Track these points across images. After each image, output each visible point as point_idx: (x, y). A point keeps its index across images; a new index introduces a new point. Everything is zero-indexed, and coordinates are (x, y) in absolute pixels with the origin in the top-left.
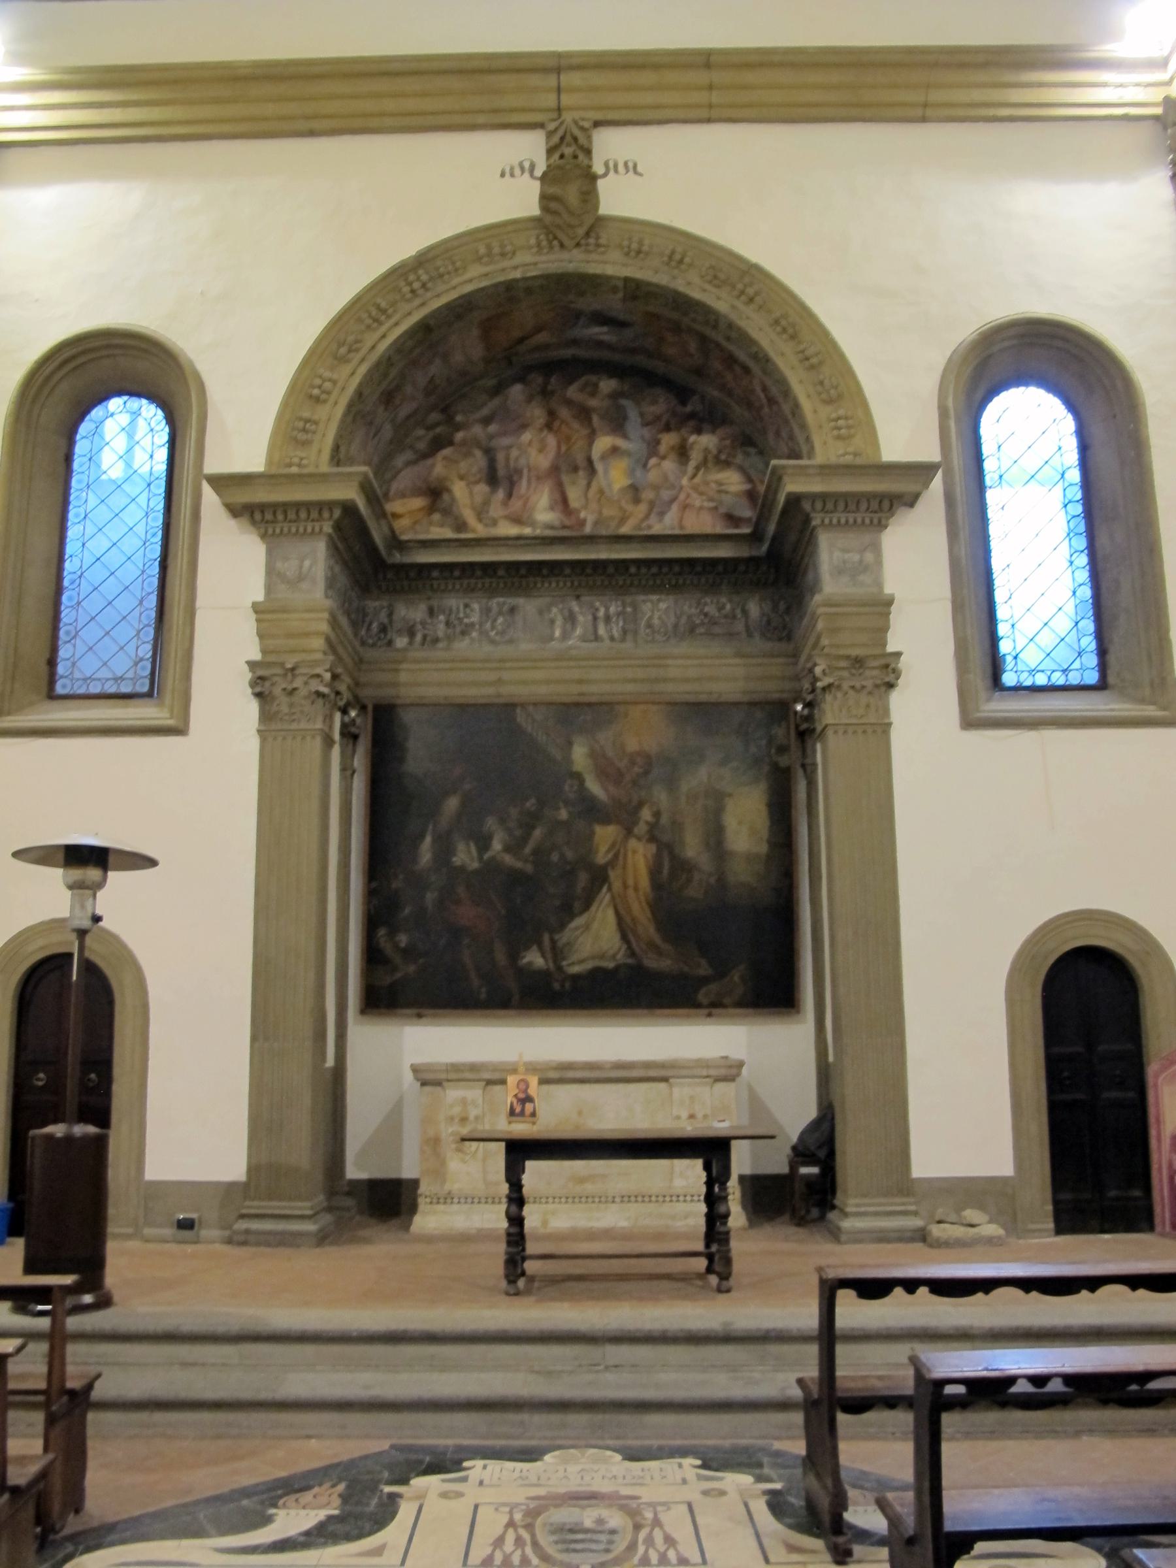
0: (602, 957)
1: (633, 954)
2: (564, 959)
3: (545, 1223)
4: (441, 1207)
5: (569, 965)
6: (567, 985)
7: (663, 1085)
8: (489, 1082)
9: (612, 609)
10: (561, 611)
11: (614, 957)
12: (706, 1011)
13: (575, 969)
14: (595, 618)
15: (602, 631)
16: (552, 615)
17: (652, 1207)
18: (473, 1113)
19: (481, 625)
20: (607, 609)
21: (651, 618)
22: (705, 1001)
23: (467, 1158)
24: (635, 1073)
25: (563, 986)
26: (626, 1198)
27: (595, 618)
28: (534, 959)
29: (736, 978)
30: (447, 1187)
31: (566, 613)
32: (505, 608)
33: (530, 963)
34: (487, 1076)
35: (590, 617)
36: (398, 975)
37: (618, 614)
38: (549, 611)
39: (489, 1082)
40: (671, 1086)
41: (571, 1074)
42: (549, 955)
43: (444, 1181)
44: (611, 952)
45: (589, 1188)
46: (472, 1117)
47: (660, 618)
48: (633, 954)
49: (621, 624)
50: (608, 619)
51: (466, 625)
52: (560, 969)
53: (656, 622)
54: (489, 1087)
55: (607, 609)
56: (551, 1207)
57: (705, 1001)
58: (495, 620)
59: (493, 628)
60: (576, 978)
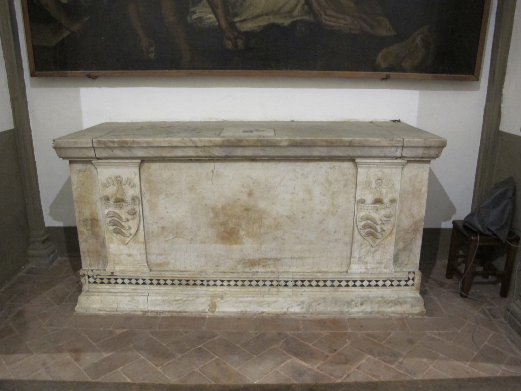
0: (276, 13)
1: (311, 10)
2: (236, 15)
3: (213, 306)
4: (105, 287)
5: (241, 21)
6: (240, 42)
7: (347, 165)
8: (143, 160)
11: (291, 12)
12: (384, 74)
13: (249, 26)
17: (327, 292)
18: (131, 192)
22: (383, 65)
23: (128, 239)
24: (316, 152)
25: (236, 45)
26: (299, 283)
28: (205, 15)
29: (418, 41)
30: (109, 268)
33: (200, 19)
34: (141, 153)
36: (66, 33)
39: (143, 160)
40: (356, 165)
41: (239, 152)
42: (220, 11)
43: (105, 261)
44: (287, 8)
45: (261, 272)
46: (128, 199)
48: (311, 10)
52: (232, 25)
54: (146, 165)
56: (219, 290)
57: (383, 65)
60: (248, 35)
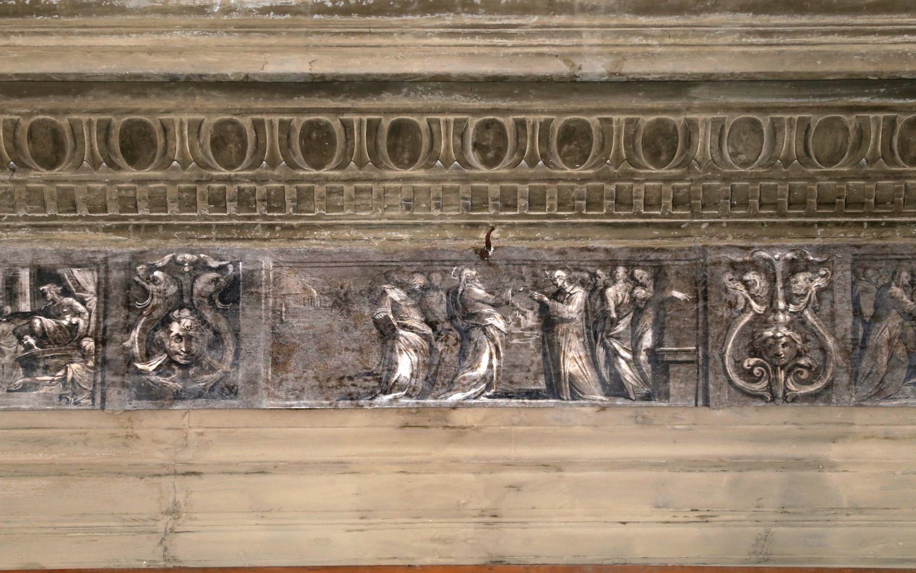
9: (615, 293)
10: (420, 298)
14: (549, 322)
15: (574, 361)
16: (384, 311)
19: (102, 342)
20: (596, 292)
21: (761, 321)
27: (549, 322)
31: (438, 303)
32: (203, 283)
35: (531, 319)
37: (637, 309)
38: (377, 297)
47: (797, 323)
49: (648, 340)
50: (597, 325)
51: (43, 337)
53: (780, 331)
55: (596, 292)
58: (166, 322)
59: (150, 349)
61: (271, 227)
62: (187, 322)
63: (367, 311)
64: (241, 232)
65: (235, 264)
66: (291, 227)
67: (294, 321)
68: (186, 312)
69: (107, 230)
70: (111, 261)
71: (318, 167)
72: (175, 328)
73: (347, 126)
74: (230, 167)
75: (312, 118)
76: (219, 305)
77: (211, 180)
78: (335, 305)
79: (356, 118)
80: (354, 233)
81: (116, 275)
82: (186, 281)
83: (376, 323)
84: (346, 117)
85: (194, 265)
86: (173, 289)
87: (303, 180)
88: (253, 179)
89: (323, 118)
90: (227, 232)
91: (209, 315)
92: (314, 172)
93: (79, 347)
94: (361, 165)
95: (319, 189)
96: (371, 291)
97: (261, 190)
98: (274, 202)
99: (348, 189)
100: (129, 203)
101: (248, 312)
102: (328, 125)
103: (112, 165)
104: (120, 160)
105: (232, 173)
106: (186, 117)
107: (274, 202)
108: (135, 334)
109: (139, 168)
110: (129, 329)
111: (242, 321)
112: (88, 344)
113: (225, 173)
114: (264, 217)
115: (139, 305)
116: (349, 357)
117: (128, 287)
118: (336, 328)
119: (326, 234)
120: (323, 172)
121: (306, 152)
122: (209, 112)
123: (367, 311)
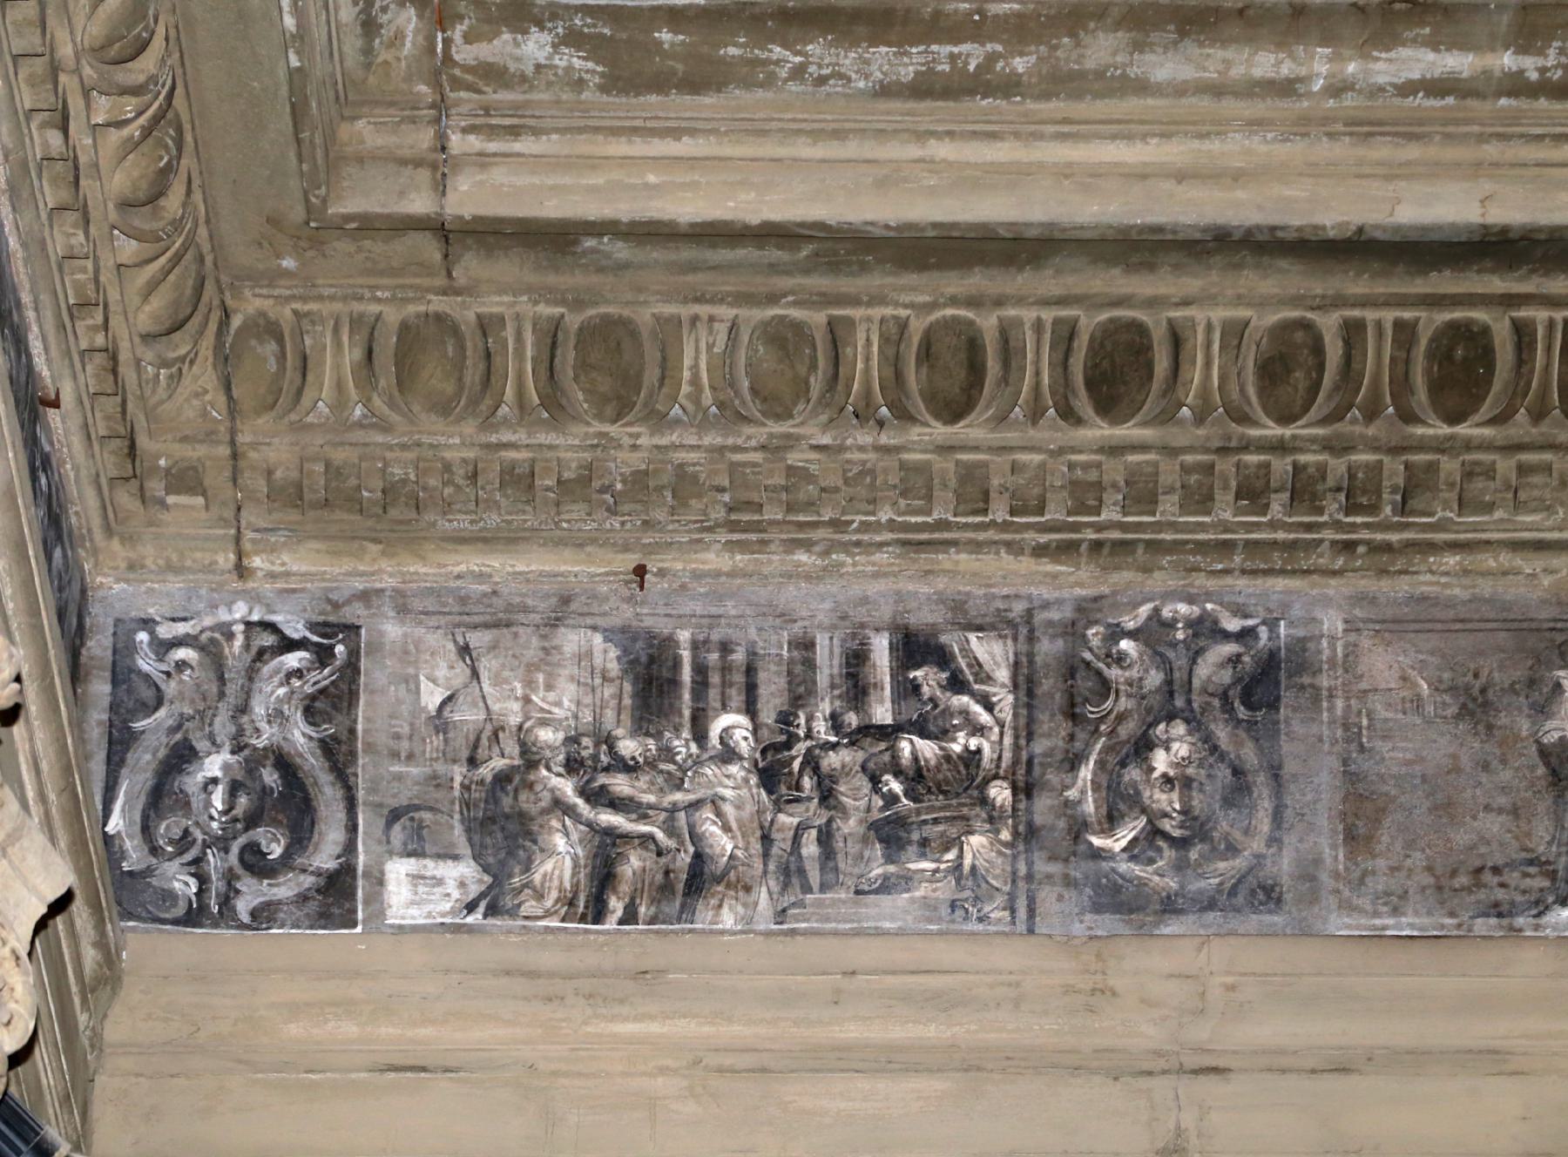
19: (1025, 790)
61: (1349, 546)
62: (1181, 749)
63: (1525, 726)
64: (1286, 557)
65: (1272, 624)
66: (1387, 548)
67: (1383, 747)
68: (1179, 728)
69: (1040, 551)
70: (1040, 617)
71: (1454, 419)
72: (1161, 761)
73: (1523, 334)
74: (1285, 419)
75: (1458, 314)
76: (1242, 712)
77: (1245, 447)
78: (1464, 712)
79: (1540, 315)
80: (1505, 559)
81: (1049, 648)
82: (1180, 660)
83: (1544, 752)
84: (1523, 313)
85: (1195, 625)
86: (1155, 679)
87: (1421, 446)
88: (1328, 446)
89: (1480, 315)
90: (1264, 557)
91: (1222, 734)
92: (1445, 430)
93: (984, 801)
94: (1538, 416)
95: (1450, 466)
96: (1532, 683)
97: (1338, 467)
98: (1359, 494)
99: (1505, 466)
100: (1086, 495)
101: (1297, 727)
102: (1486, 331)
103: (1069, 415)
104: (1083, 404)
105: (1288, 432)
106: (1219, 314)
107: (1359, 494)
108: (1086, 772)
109: (1115, 422)
110: (1073, 762)
111: (1286, 747)
112: (1000, 793)
113: (1273, 431)
114: (1338, 525)
115: (1092, 712)
116: (1494, 825)
117: (1071, 673)
118: (1465, 761)
119: (1452, 560)
120: (1462, 430)
121: (1437, 388)
122: (1262, 304)
123: (1525, 726)
